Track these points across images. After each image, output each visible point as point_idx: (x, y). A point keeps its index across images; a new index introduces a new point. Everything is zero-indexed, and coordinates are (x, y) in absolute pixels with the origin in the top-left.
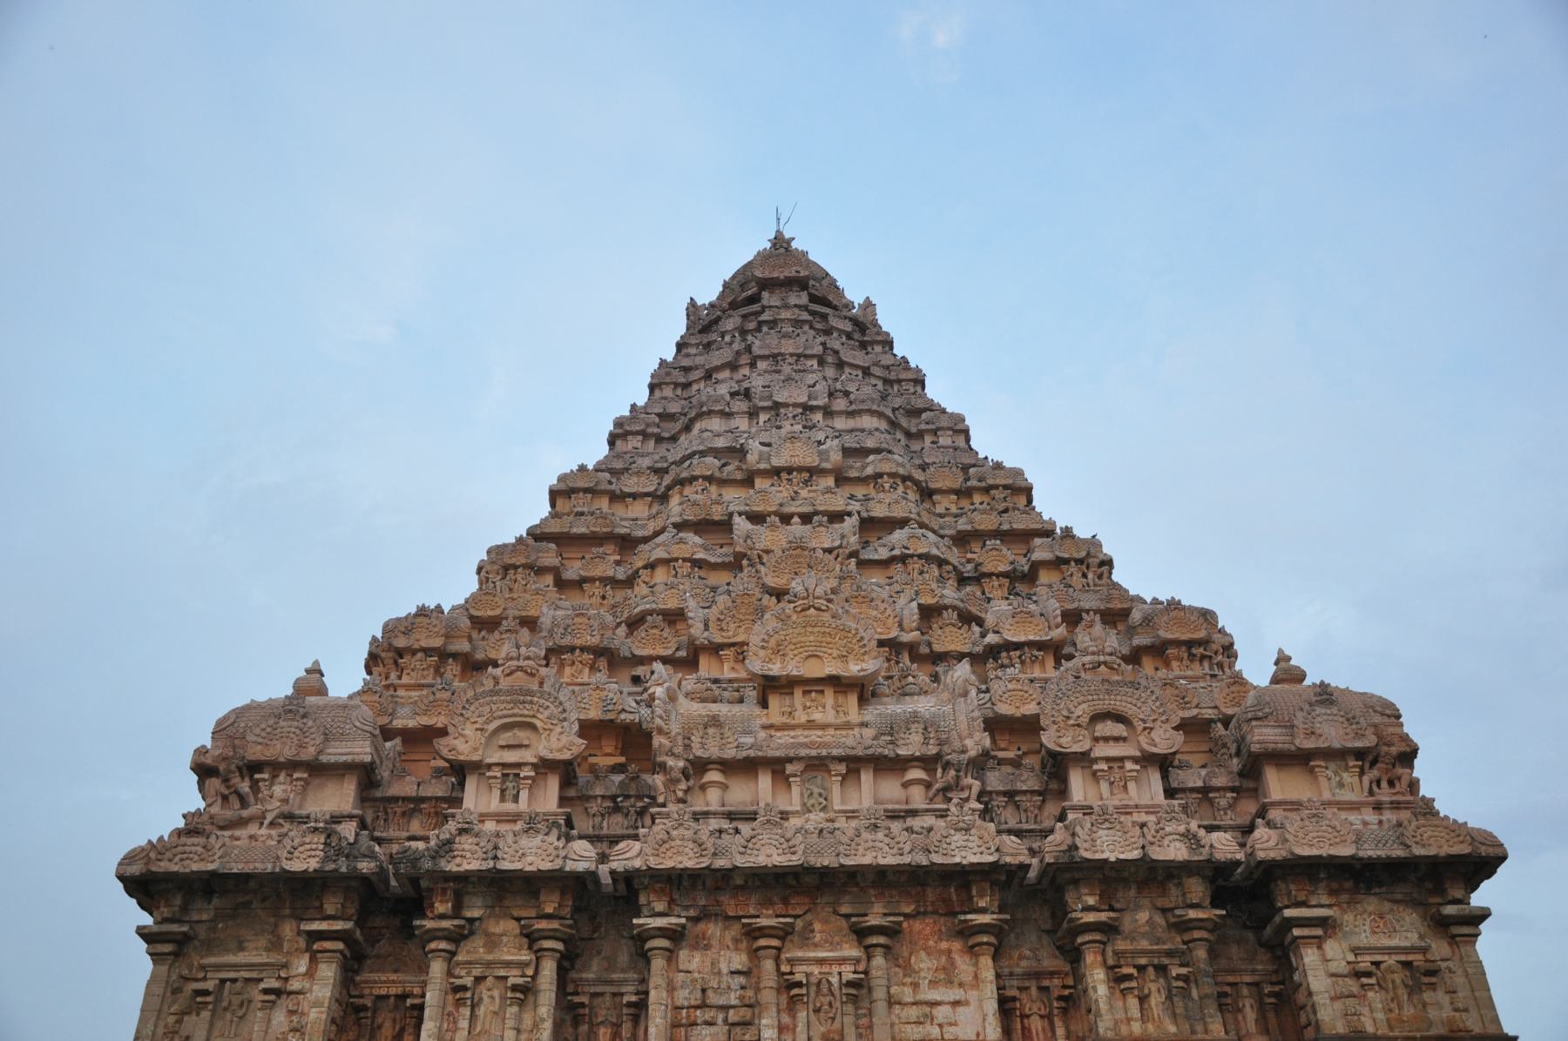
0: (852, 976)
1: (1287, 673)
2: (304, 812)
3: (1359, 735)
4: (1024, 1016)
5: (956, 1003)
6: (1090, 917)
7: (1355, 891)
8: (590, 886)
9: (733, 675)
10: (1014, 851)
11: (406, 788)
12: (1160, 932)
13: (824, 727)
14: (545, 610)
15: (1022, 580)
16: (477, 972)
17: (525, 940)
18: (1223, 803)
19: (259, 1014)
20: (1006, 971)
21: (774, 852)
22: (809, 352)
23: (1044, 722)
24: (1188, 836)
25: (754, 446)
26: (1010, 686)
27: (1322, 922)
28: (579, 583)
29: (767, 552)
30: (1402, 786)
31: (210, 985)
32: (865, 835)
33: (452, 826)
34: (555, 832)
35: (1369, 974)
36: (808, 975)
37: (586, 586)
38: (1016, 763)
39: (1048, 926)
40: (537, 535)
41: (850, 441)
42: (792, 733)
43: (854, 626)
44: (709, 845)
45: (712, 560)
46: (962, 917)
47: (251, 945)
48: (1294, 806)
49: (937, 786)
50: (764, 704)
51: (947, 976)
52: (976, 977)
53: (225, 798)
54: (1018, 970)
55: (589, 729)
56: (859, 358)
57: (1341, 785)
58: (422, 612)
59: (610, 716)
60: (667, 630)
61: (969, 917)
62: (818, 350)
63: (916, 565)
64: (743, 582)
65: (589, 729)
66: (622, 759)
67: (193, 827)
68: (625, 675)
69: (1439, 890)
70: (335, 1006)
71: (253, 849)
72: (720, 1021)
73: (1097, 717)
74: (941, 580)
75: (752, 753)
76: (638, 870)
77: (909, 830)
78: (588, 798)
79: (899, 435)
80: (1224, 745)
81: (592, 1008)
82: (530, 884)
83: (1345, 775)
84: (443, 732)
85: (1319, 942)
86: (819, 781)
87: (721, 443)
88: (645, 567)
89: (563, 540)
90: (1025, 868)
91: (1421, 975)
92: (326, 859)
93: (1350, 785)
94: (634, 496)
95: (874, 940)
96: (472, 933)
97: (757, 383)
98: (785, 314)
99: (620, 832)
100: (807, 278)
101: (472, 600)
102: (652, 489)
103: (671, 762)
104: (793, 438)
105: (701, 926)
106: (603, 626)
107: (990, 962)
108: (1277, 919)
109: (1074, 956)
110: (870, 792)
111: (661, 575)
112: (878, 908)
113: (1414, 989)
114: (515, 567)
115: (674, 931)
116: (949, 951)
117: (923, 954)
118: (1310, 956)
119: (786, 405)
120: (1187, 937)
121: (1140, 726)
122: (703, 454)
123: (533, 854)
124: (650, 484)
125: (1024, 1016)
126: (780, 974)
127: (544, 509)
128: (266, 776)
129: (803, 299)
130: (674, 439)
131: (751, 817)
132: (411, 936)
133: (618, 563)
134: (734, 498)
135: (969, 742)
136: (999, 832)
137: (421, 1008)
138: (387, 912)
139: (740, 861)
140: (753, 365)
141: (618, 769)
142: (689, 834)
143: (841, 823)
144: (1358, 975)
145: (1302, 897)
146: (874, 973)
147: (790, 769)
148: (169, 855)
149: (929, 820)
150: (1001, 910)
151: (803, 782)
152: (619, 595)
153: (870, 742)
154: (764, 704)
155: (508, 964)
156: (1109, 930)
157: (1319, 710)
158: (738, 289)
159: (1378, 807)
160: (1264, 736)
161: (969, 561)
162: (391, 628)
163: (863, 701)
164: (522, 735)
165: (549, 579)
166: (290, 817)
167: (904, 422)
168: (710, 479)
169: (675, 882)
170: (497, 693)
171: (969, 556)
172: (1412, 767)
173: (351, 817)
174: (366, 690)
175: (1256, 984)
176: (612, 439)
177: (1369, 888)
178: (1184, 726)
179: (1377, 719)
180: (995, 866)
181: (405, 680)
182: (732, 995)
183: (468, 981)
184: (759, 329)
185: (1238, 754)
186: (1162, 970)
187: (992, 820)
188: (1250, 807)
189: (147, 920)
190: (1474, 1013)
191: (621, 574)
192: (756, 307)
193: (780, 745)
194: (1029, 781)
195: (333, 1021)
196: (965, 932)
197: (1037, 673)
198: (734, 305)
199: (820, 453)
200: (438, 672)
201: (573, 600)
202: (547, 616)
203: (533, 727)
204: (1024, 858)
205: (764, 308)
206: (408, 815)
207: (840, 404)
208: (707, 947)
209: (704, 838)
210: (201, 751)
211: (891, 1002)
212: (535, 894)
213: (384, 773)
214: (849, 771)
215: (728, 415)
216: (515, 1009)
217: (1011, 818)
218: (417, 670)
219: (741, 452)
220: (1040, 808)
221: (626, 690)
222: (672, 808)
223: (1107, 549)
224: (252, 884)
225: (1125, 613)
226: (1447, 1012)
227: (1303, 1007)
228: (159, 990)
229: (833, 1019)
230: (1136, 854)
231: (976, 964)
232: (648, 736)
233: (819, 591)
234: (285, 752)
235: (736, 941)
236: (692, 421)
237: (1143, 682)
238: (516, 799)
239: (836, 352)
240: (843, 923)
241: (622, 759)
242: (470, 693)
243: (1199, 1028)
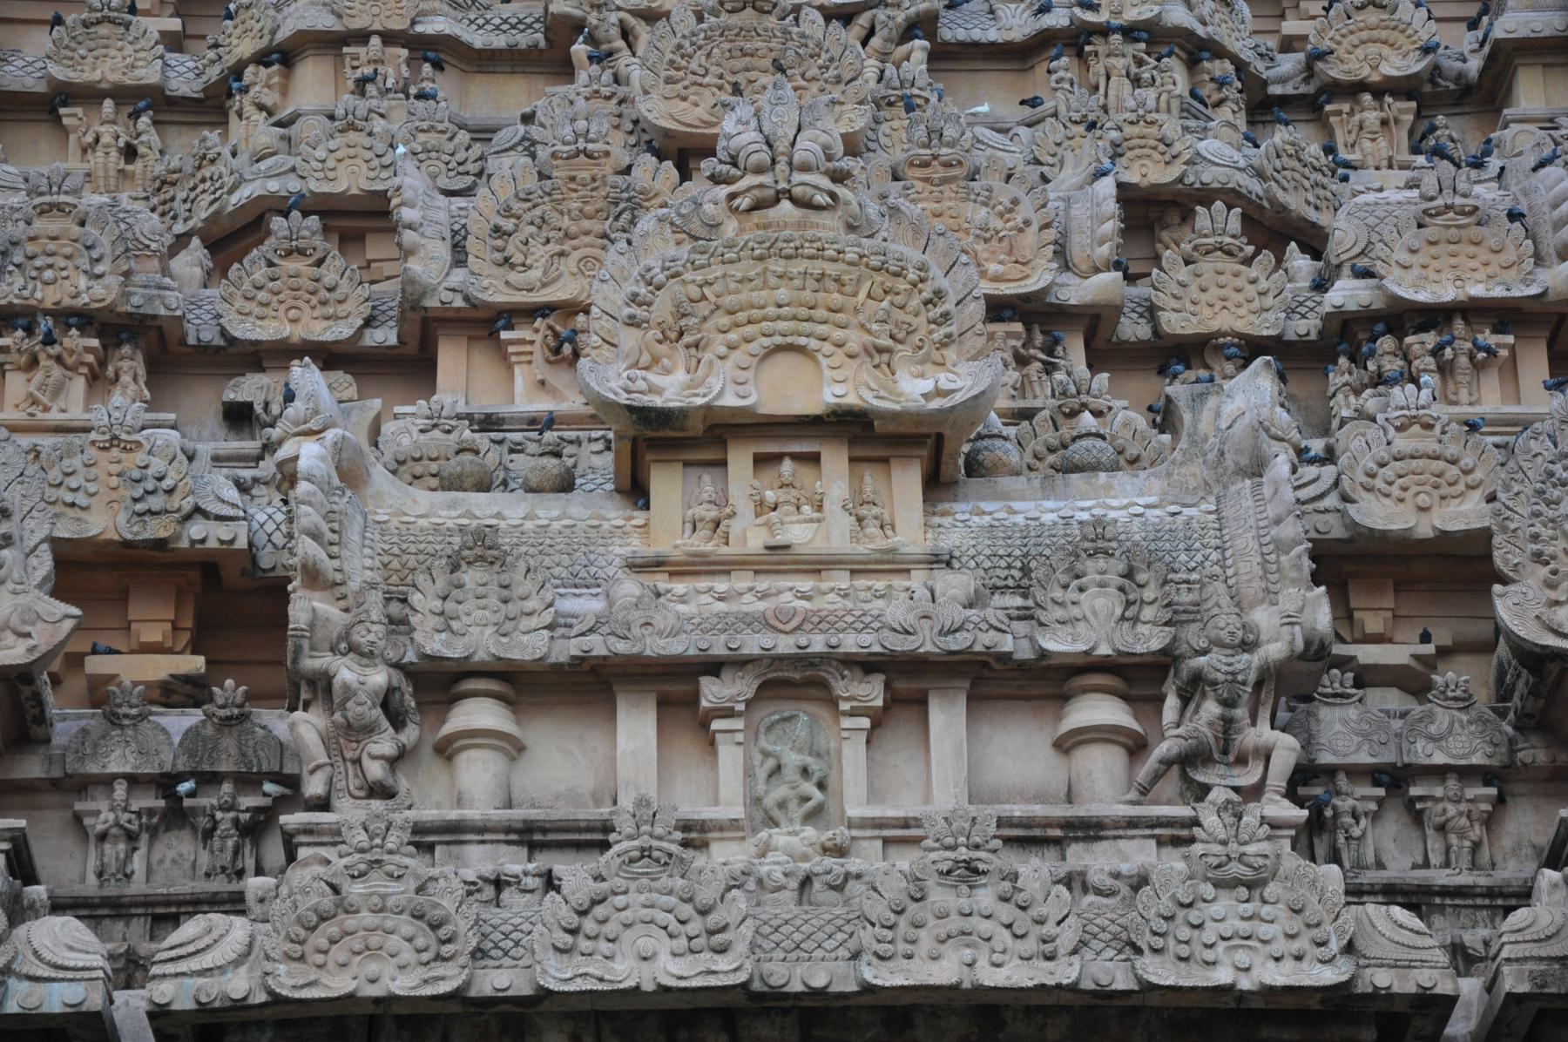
9: (543, 405)
13: (817, 566)
21: (664, 945)
26: (1402, 443)
29: (651, 16)
32: (941, 896)
37: (71, 115)
38: (1413, 681)
42: (721, 585)
43: (914, 255)
44: (461, 924)
45: (478, 40)
59: (156, 529)
60: (336, 262)
63: (1115, 58)
64: (566, 109)
65: (87, 572)
66: (195, 663)
68: (203, 400)
74: (1197, 106)
75: (597, 645)
76: (239, 1006)
77: (1074, 881)
78: (83, 785)
86: (800, 729)
88: (262, 59)
99: (186, 886)
103: (346, 672)
106: (131, 248)
110: (959, 764)
111: (313, 86)
131: (592, 838)
133: (174, 42)
135: (1263, 618)
136: (1356, 893)
139: (559, 975)
142: (400, 892)
143: (868, 858)
147: (712, 692)
149: (1138, 854)
151: (753, 733)
152: (182, 147)
153: (958, 614)
154: (635, 491)
161: (1288, 44)
163: (936, 485)
171: (1290, 27)
187: (1335, 858)
191: (185, 77)
193: (682, 620)
197: (1490, 400)
209: (448, 904)
214: (894, 701)
217: (1394, 850)
221: (205, 449)
222: (349, 812)
232: (276, 592)
241: (195, 663)
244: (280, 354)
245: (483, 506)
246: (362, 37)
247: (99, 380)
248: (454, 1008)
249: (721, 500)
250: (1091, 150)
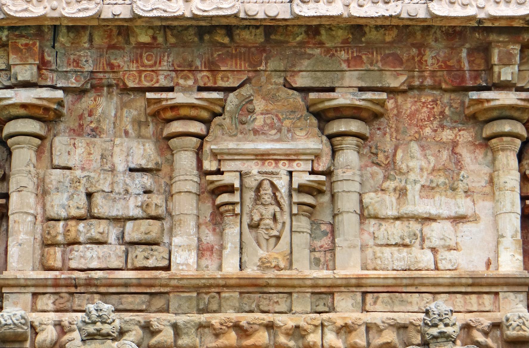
5: (459, 219)
46: (474, 95)
52: (491, 181)
61: (485, 95)
72: (112, 238)
105: (87, 101)
107: (514, 162)
112: (352, 78)
115: (47, 109)
116: (455, 144)
117: (415, 147)
126: (204, 173)
146: (339, 174)
182: (132, 202)
196: (478, 118)
208: (96, 132)
229: (278, 238)
235: (139, 123)
240: (298, 97)
248: (95, 23)
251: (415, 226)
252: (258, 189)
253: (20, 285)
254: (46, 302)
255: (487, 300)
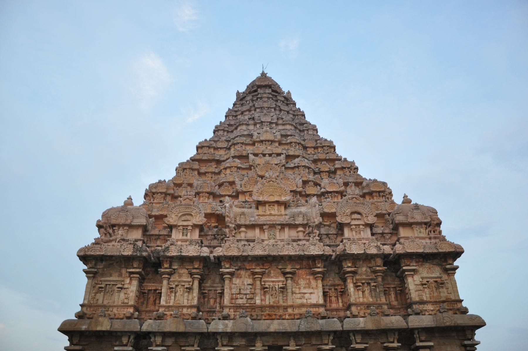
0: (282, 286)
1: (406, 200)
2: (127, 239)
3: (426, 218)
4: (330, 297)
5: (311, 293)
6: (349, 269)
7: (423, 262)
8: (208, 260)
10: (328, 251)
11: (156, 232)
12: (369, 274)
13: (274, 215)
14: (195, 181)
15: (332, 173)
16: (176, 284)
17: (189, 275)
18: (388, 237)
19: (117, 294)
20: (325, 284)
21: (260, 251)
22: (271, 106)
23: (337, 214)
24: (377, 247)
25: (255, 134)
26: (328, 204)
27: (414, 270)
28: (205, 173)
29: (259, 165)
30: (437, 232)
31: (103, 286)
32: (286, 246)
33: (169, 243)
34: (198, 245)
35: (425, 284)
36: (269, 285)
38: (329, 226)
39: (337, 272)
40: (193, 159)
41: (283, 133)
44: (241, 249)
45: (243, 167)
47: (114, 275)
48: (407, 238)
49: (307, 232)
50: (257, 208)
51: (309, 286)
52: (317, 286)
53: (105, 234)
54: (329, 284)
55: (207, 216)
56: (286, 108)
57: (420, 232)
58: (160, 182)
59: (213, 212)
62: (274, 106)
63: (301, 169)
64: (251, 173)
65: (207, 216)
66: (217, 224)
67: (97, 242)
68: (218, 200)
69: (446, 261)
70: (137, 292)
71: (113, 249)
73: (353, 213)
74: (309, 173)
75: (254, 223)
76: (221, 256)
78: (207, 235)
79: (297, 131)
80: (388, 221)
81: (208, 294)
82: (191, 260)
83: (422, 229)
84: (166, 216)
85: (412, 276)
87: (246, 133)
88: (224, 169)
89: (200, 161)
90: (331, 256)
91: (439, 284)
92: (134, 252)
93: (423, 232)
94: (221, 148)
95: (288, 276)
96: (175, 273)
97: (256, 115)
98: (265, 95)
99: (216, 245)
100: (271, 85)
101: (174, 178)
102: (225, 146)
103: (231, 225)
104: (266, 131)
105: (239, 272)
106: (212, 186)
107: (321, 282)
108: (401, 270)
109: (345, 280)
110: (288, 234)
111: (228, 171)
112: (289, 267)
113: (437, 288)
114: (186, 169)
116: (309, 279)
117: (302, 280)
118: (410, 280)
119: (265, 122)
120: (376, 275)
121: (364, 215)
122: (240, 136)
123: (192, 251)
124: (225, 145)
125: (330, 297)
126: (262, 285)
127: (195, 152)
128: (117, 228)
129: (270, 91)
130: (232, 132)
131: (253, 241)
132: (158, 273)
133: (216, 168)
134: (250, 149)
135: (316, 220)
136: (324, 245)
137: (161, 293)
138: (151, 267)
140: (255, 110)
141: (216, 227)
142: (236, 246)
143: (279, 243)
144: (423, 285)
145: (408, 264)
146: (288, 285)
147: (265, 227)
148: (91, 250)
149: (304, 242)
150: (324, 268)
152: (216, 177)
154: (257, 208)
155: (185, 282)
156: (355, 273)
157: (415, 211)
158: (251, 88)
159: (430, 238)
160: (399, 218)
161: (317, 168)
162: (151, 186)
163: (286, 208)
164: (188, 217)
165: (196, 173)
166: (123, 240)
167: (299, 127)
168: (242, 143)
169: (232, 259)
170: (181, 205)
172: (440, 227)
173: (140, 240)
174: (144, 204)
175: (395, 288)
176: (214, 132)
177: (427, 261)
178: (377, 216)
179: (431, 214)
180: (322, 255)
181: (155, 201)
183: (174, 286)
184: (257, 100)
185: (392, 223)
186: (369, 284)
188: (395, 238)
189: (85, 267)
190: (453, 294)
191: (217, 171)
192: (256, 93)
193: (262, 220)
194: (333, 231)
195: (137, 296)
196: (314, 274)
197: (336, 200)
198: (250, 93)
199: (274, 136)
200: (164, 199)
201: (204, 178)
202: (195, 183)
203: (191, 215)
204: (331, 253)
205: (258, 94)
206: (156, 240)
207: (280, 122)
208: (241, 277)
210: (99, 221)
211: (293, 293)
212: (192, 262)
213: (149, 228)
214: (281, 228)
215: (248, 125)
216: (187, 294)
217: (327, 241)
218: (158, 198)
219: (251, 136)
220: (336, 239)
222: (231, 238)
223: (357, 164)
224: (114, 258)
225: (361, 183)
226: (446, 294)
227: (407, 294)
228: (89, 286)
230: (362, 252)
231: (317, 282)
232: (224, 217)
233: (273, 176)
234: (122, 221)
235: (249, 276)
236: (237, 127)
237: (366, 203)
238: (187, 235)
239: (279, 107)
240: (279, 271)
241: (217, 224)
242: (173, 205)
243: (379, 299)
244: (225, 196)
245: (243, 210)
246: (232, 167)
247: (209, 198)
249: (265, 209)
250: (299, 177)
251: (303, 295)
252: (272, 288)
253: (227, 307)
254: (232, 310)
255: (317, 309)
